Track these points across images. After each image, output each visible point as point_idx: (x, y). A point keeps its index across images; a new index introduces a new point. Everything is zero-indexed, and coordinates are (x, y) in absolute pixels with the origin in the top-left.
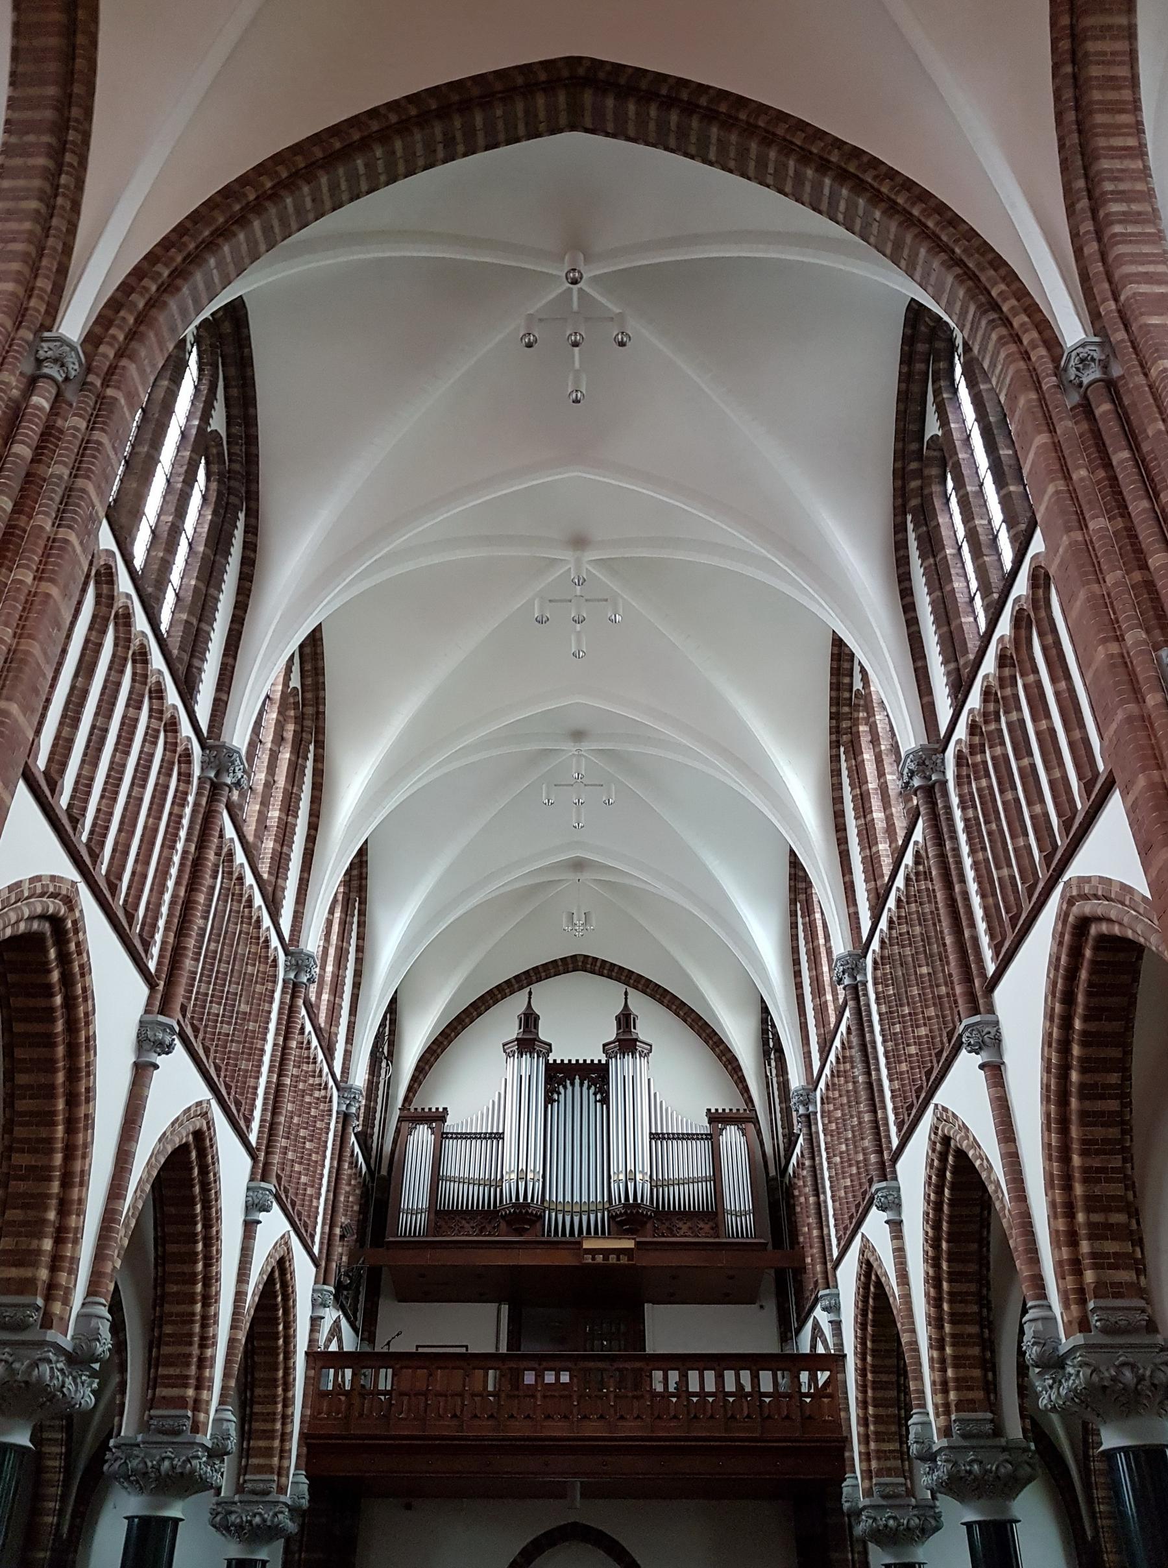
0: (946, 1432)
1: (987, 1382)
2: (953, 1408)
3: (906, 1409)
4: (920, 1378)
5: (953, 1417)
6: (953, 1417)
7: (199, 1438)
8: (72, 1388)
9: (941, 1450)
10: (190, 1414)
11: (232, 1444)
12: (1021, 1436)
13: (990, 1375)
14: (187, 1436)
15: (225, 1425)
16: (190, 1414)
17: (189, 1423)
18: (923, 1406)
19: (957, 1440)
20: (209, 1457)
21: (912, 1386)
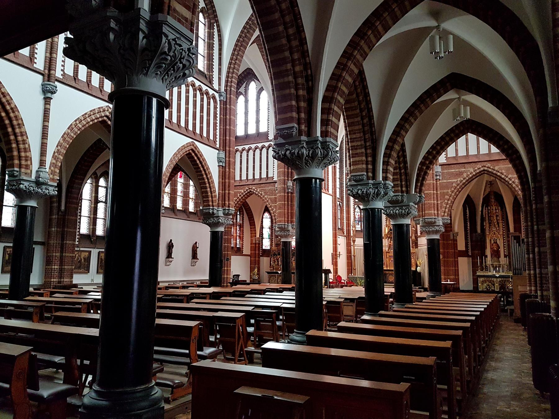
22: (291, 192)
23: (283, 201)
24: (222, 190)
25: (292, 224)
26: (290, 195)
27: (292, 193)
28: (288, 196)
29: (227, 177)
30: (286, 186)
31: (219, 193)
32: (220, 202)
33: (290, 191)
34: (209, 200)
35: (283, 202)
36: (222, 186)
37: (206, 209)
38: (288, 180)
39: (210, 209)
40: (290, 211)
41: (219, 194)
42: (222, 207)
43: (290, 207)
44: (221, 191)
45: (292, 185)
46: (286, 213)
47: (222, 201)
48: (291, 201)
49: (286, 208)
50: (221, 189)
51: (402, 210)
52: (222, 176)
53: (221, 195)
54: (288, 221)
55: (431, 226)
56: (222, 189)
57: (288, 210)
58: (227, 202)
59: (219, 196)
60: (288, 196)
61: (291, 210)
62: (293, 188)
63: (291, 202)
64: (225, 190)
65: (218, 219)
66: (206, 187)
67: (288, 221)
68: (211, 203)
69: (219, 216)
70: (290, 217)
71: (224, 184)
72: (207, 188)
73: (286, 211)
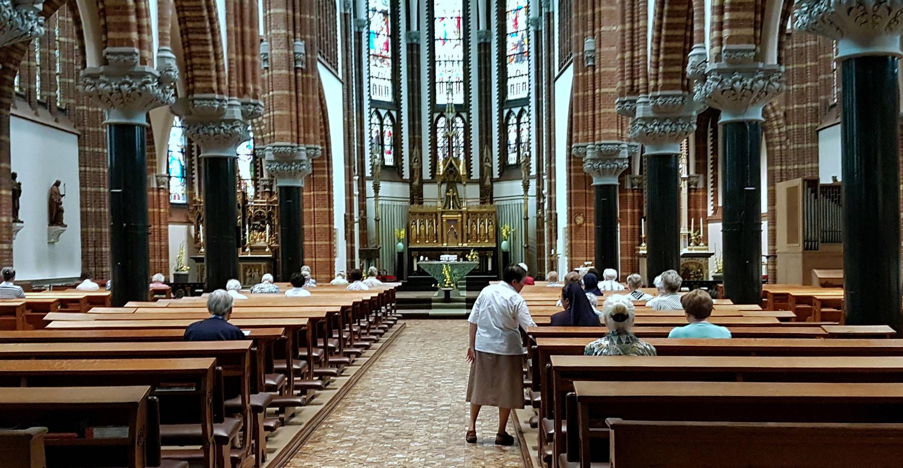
0: (718, 58)
1: (756, 22)
2: (724, 42)
3: (688, 42)
4: (702, 21)
5: (724, 48)
6: (724, 48)
7: (147, 68)
8: (19, 20)
9: (711, 71)
10: (137, 50)
11: (175, 73)
12: (776, 62)
13: (759, 16)
14: (138, 67)
15: (168, 61)
16: (137, 50)
17: (137, 58)
18: (702, 40)
19: (723, 65)
20: (160, 84)
21: (696, 27)
24: (237, 54)
25: (308, 146)
28: (296, 77)
29: (247, 20)
30: (291, 52)
31: (230, 60)
32: (234, 83)
34: (211, 77)
35: (287, 92)
36: (236, 42)
37: (204, 99)
38: (295, 37)
39: (213, 99)
40: (301, 115)
41: (230, 64)
42: (239, 96)
43: (301, 105)
44: (234, 56)
46: (294, 118)
47: (238, 82)
49: (294, 108)
50: (234, 49)
51: (677, 125)
52: (235, 17)
53: (234, 66)
54: (298, 138)
56: (237, 49)
57: (297, 112)
58: (250, 86)
59: (230, 68)
60: (296, 77)
62: (307, 58)
64: (244, 54)
65: (233, 128)
66: (206, 40)
67: (298, 138)
68: (214, 85)
69: (234, 120)
71: (239, 37)
72: (207, 45)
73: (294, 113)
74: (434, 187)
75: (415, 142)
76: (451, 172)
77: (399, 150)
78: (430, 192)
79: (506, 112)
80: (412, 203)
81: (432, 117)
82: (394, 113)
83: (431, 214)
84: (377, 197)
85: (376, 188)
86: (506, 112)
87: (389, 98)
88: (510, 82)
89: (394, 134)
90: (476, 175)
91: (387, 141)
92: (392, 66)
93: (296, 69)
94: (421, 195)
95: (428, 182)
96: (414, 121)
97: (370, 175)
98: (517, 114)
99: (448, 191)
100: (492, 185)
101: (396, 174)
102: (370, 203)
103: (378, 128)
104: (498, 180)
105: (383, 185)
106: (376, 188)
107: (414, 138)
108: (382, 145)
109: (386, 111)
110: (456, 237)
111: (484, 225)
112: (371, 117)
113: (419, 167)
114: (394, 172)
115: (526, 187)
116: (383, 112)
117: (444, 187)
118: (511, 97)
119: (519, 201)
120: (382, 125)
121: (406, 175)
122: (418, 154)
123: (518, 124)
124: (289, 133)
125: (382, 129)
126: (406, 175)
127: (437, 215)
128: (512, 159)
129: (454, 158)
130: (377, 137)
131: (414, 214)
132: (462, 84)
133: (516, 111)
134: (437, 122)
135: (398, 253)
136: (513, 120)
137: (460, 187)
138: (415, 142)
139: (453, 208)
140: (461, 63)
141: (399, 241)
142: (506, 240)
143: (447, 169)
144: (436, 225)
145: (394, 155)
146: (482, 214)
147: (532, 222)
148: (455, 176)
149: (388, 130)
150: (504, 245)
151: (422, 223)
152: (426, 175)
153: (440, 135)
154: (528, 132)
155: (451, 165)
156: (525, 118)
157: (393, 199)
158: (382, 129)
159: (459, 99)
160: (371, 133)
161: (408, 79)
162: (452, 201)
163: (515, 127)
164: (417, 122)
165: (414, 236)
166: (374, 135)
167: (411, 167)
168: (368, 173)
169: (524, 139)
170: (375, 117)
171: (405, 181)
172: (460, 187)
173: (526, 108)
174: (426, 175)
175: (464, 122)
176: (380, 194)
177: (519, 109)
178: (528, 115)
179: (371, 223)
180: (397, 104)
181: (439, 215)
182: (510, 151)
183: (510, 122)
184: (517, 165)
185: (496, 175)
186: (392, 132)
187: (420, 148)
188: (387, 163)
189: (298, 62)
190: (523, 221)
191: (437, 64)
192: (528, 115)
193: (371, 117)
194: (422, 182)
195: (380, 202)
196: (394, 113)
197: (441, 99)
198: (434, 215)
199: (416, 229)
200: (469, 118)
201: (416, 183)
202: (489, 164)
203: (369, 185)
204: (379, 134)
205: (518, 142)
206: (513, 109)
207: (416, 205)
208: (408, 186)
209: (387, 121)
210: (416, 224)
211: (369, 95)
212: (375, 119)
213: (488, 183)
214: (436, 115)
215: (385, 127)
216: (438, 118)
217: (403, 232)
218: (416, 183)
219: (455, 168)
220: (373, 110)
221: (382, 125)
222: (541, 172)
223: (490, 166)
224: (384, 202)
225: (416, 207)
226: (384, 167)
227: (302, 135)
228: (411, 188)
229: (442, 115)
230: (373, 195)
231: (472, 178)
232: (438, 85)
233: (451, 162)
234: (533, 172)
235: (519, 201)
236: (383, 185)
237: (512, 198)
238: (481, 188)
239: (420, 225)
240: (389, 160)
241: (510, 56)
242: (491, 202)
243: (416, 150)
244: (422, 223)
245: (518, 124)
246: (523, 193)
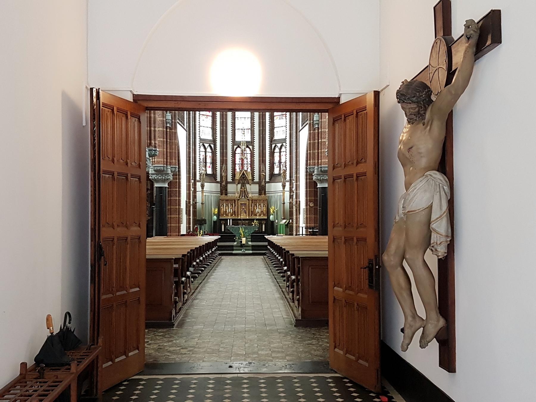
22: (170, 127)
23: (162, 137)
25: (171, 166)
26: (168, 130)
27: (170, 129)
28: (167, 131)
30: (165, 119)
33: (168, 125)
35: (162, 139)
40: (168, 151)
43: (168, 145)
45: (171, 119)
46: (165, 152)
48: (170, 138)
49: (165, 146)
54: (167, 162)
55: (325, 174)
57: (167, 149)
60: (167, 131)
61: (170, 150)
62: (172, 122)
63: (170, 140)
67: (167, 162)
70: (169, 158)
73: (165, 150)
74: (234, 185)
75: (224, 161)
76: (243, 177)
77: (215, 165)
78: (231, 188)
79: (273, 146)
80: (222, 194)
81: (233, 148)
82: (212, 146)
83: (231, 200)
84: (203, 191)
85: (203, 186)
86: (273, 146)
87: (210, 138)
88: (275, 130)
89: (212, 157)
90: (257, 179)
91: (209, 160)
92: (212, 120)
93: (167, 127)
94: (226, 190)
95: (230, 183)
96: (223, 150)
97: (199, 179)
98: (279, 147)
99: (241, 188)
100: (265, 185)
101: (213, 179)
102: (199, 195)
103: (204, 153)
104: (268, 182)
105: (206, 184)
106: (203, 186)
107: (223, 159)
108: (206, 163)
109: (208, 144)
110: (246, 213)
111: (261, 206)
112: (200, 148)
113: (225, 175)
114: (212, 177)
115: (284, 186)
116: (206, 145)
117: (239, 186)
118: (276, 137)
119: (280, 194)
120: (206, 152)
121: (219, 179)
122: (225, 168)
123: (280, 152)
124: (162, 160)
125: (206, 154)
126: (219, 179)
127: (235, 201)
128: (276, 171)
129: (245, 170)
130: (203, 159)
131: (223, 200)
132: (250, 130)
133: (279, 145)
134: (235, 150)
135: (214, 222)
136: (277, 150)
137: (248, 186)
138: (224, 161)
139: (244, 197)
140: (250, 119)
141: (215, 215)
142: (273, 215)
143: (241, 176)
144: (235, 206)
145: (212, 168)
146: (260, 200)
147: (287, 205)
148: (245, 180)
149: (209, 155)
150: (271, 217)
151: (227, 205)
152: (230, 179)
153: (238, 157)
154: (285, 157)
155: (243, 174)
156: (283, 149)
157: (211, 192)
158: (206, 154)
159: (249, 139)
160: (199, 156)
161: (220, 127)
162: (244, 193)
163: (278, 154)
164: (225, 151)
165: (222, 212)
166: (202, 157)
167: (221, 174)
168: (198, 178)
169: (283, 160)
170: (202, 148)
171: (218, 182)
172: (248, 186)
173: (284, 144)
174: (230, 179)
175: (251, 150)
176: (204, 190)
177: (281, 144)
178: (286, 148)
179: (199, 205)
180: (214, 141)
181: (236, 201)
182: (275, 167)
183: (276, 151)
184: (279, 174)
185: (267, 180)
186: (211, 156)
187: (226, 165)
188: (208, 173)
189: (168, 124)
190: (282, 204)
191: (236, 119)
192: (286, 148)
193: (200, 148)
194: (227, 183)
195: (204, 194)
196: (212, 146)
197: (238, 139)
198: (233, 201)
199: (223, 209)
200: (253, 148)
201: (224, 183)
202: (264, 174)
203: (199, 184)
204: (204, 157)
205: (280, 162)
206: (277, 144)
207: (223, 195)
208: (219, 185)
209: (209, 150)
210: (223, 206)
211: (199, 136)
212: (202, 149)
213: (263, 183)
214: (235, 147)
215: (207, 153)
216: (236, 148)
217: (216, 210)
218: (224, 183)
219: (245, 176)
220: (201, 144)
221: (206, 152)
222: (292, 179)
223: (265, 174)
224: (206, 194)
225: (223, 197)
226: (207, 175)
227: (169, 161)
228: (221, 186)
229: (239, 147)
230: (201, 190)
231: (254, 181)
232: (236, 131)
233: (243, 172)
234: (288, 178)
235: (280, 194)
236: (206, 184)
237: (275, 192)
238: (259, 186)
239: (226, 206)
240: (209, 171)
241: (276, 116)
242: (265, 194)
243: (224, 165)
244: (227, 205)
245: (280, 152)
246: (282, 189)
